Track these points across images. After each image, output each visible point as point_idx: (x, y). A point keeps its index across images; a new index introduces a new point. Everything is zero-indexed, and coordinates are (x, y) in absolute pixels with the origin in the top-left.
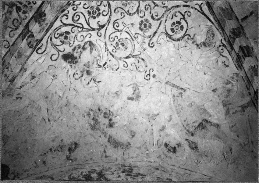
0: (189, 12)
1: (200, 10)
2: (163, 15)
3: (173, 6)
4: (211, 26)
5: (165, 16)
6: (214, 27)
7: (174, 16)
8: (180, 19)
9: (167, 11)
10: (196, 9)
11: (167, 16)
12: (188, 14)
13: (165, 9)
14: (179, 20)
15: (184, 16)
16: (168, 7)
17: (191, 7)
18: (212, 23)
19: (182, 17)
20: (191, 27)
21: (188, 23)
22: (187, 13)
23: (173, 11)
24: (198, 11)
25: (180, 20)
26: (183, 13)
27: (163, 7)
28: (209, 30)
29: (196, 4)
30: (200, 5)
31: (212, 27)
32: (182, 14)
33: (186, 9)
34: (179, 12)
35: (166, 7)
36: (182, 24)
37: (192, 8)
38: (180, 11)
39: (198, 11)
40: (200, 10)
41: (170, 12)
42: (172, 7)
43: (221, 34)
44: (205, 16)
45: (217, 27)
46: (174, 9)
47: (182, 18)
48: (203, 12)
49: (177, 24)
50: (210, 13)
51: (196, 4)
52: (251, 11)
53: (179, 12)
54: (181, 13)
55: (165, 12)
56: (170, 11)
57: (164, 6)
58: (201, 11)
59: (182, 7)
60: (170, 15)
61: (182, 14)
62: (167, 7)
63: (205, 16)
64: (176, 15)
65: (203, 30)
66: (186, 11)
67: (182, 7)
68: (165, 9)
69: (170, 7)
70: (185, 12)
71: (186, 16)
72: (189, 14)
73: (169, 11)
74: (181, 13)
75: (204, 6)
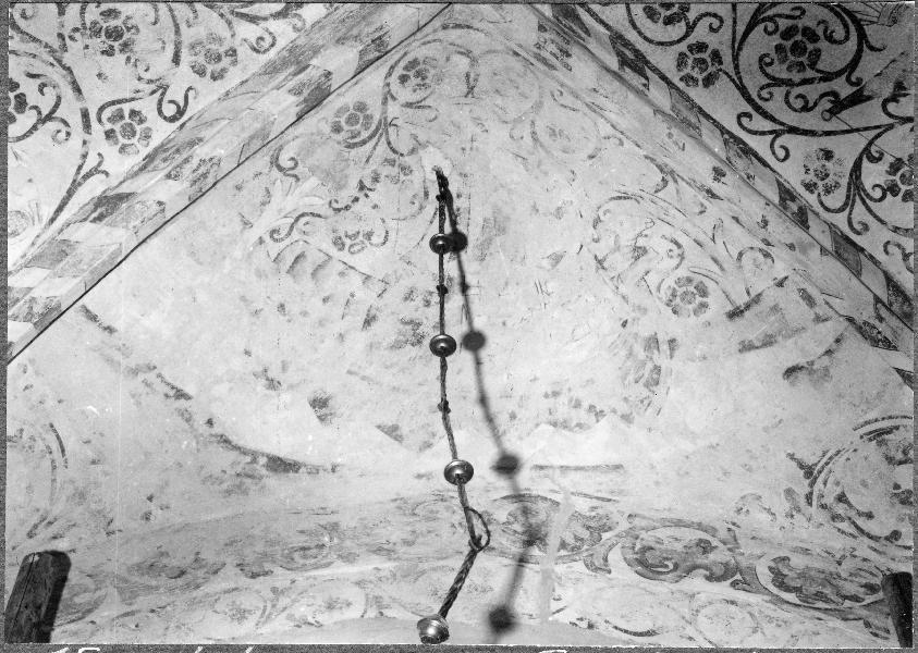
0: (68, 134)
1: (83, 172)
2: (35, 40)
3: (75, 72)
4: (40, 220)
5: (32, 47)
6: (37, 229)
7: (39, 81)
8: (35, 107)
9: (52, 51)
10: (84, 156)
11: (35, 56)
12: (59, 131)
13: (56, 44)
14: (31, 101)
15: (49, 117)
16: (66, 55)
17: (87, 137)
18: (52, 220)
19: (45, 112)
20: (19, 152)
21: (29, 140)
22: (64, 130)
23: (56, 74)
24: (80, 168)
25: (30, 108)
26: (57, 114)
27: (61, 36)
28: (23, 215)
29: (99, 155)
30: (102, 168)
31: (36, 222)
32: (53, 111)
33: (76, 121)
34: (59, 98)
35: (64, 48)
36: (18, 116)
37: (85, 143)
38: (63, 100)
39: (80, 168)
40: (83, 172)
41: (51, 64)
42: (69, 69)
43: (22, 257)
44: (70, 193)
45: (40, 241)
46: (64, 77)
47: (40, 113)
48: (80, 184)
49: (16, 97)
50: (81, 208)
51: (99, 155)
52: (115, 325)
53: (59, 98)
54: (57, 105)
55: (46, 46)
56: (55, 63)
57: (67, 39)
58: (81, 176)
59: (79, 105)
60: (38, 68)
61: (53, 111)
62: (66, 51)
63: (70, 193)
64: (45, 90)
65: (20, 195)
66: (69, 121)
67: (79, 105)
68: (56, 44)
69: (67, 59)
70: (65, 118)
71: (51, 126)
72: (62, 135)
73: (51, 60)
74: (57, 105)
75: (102, 181)
